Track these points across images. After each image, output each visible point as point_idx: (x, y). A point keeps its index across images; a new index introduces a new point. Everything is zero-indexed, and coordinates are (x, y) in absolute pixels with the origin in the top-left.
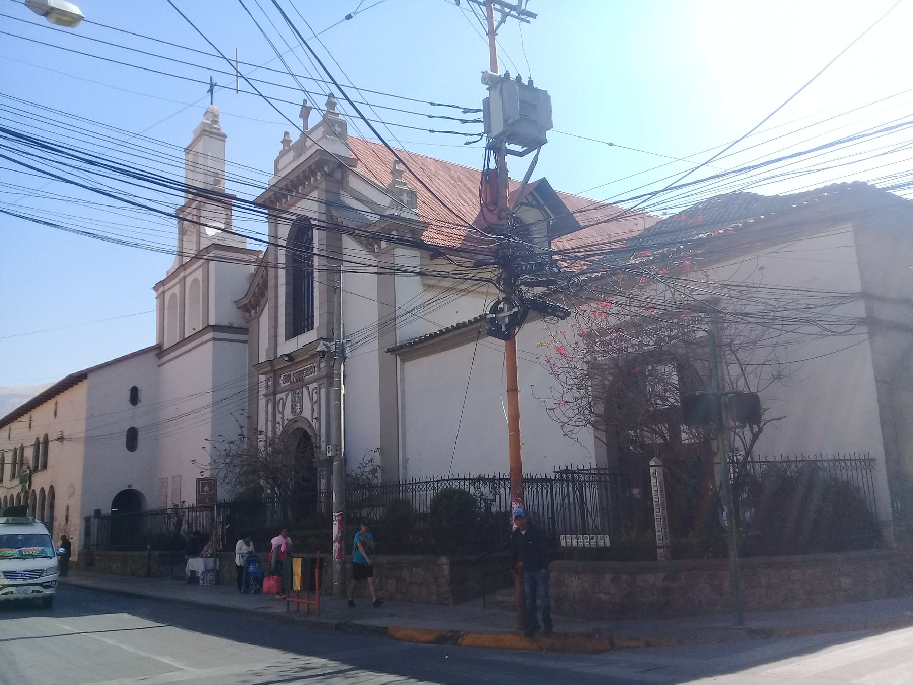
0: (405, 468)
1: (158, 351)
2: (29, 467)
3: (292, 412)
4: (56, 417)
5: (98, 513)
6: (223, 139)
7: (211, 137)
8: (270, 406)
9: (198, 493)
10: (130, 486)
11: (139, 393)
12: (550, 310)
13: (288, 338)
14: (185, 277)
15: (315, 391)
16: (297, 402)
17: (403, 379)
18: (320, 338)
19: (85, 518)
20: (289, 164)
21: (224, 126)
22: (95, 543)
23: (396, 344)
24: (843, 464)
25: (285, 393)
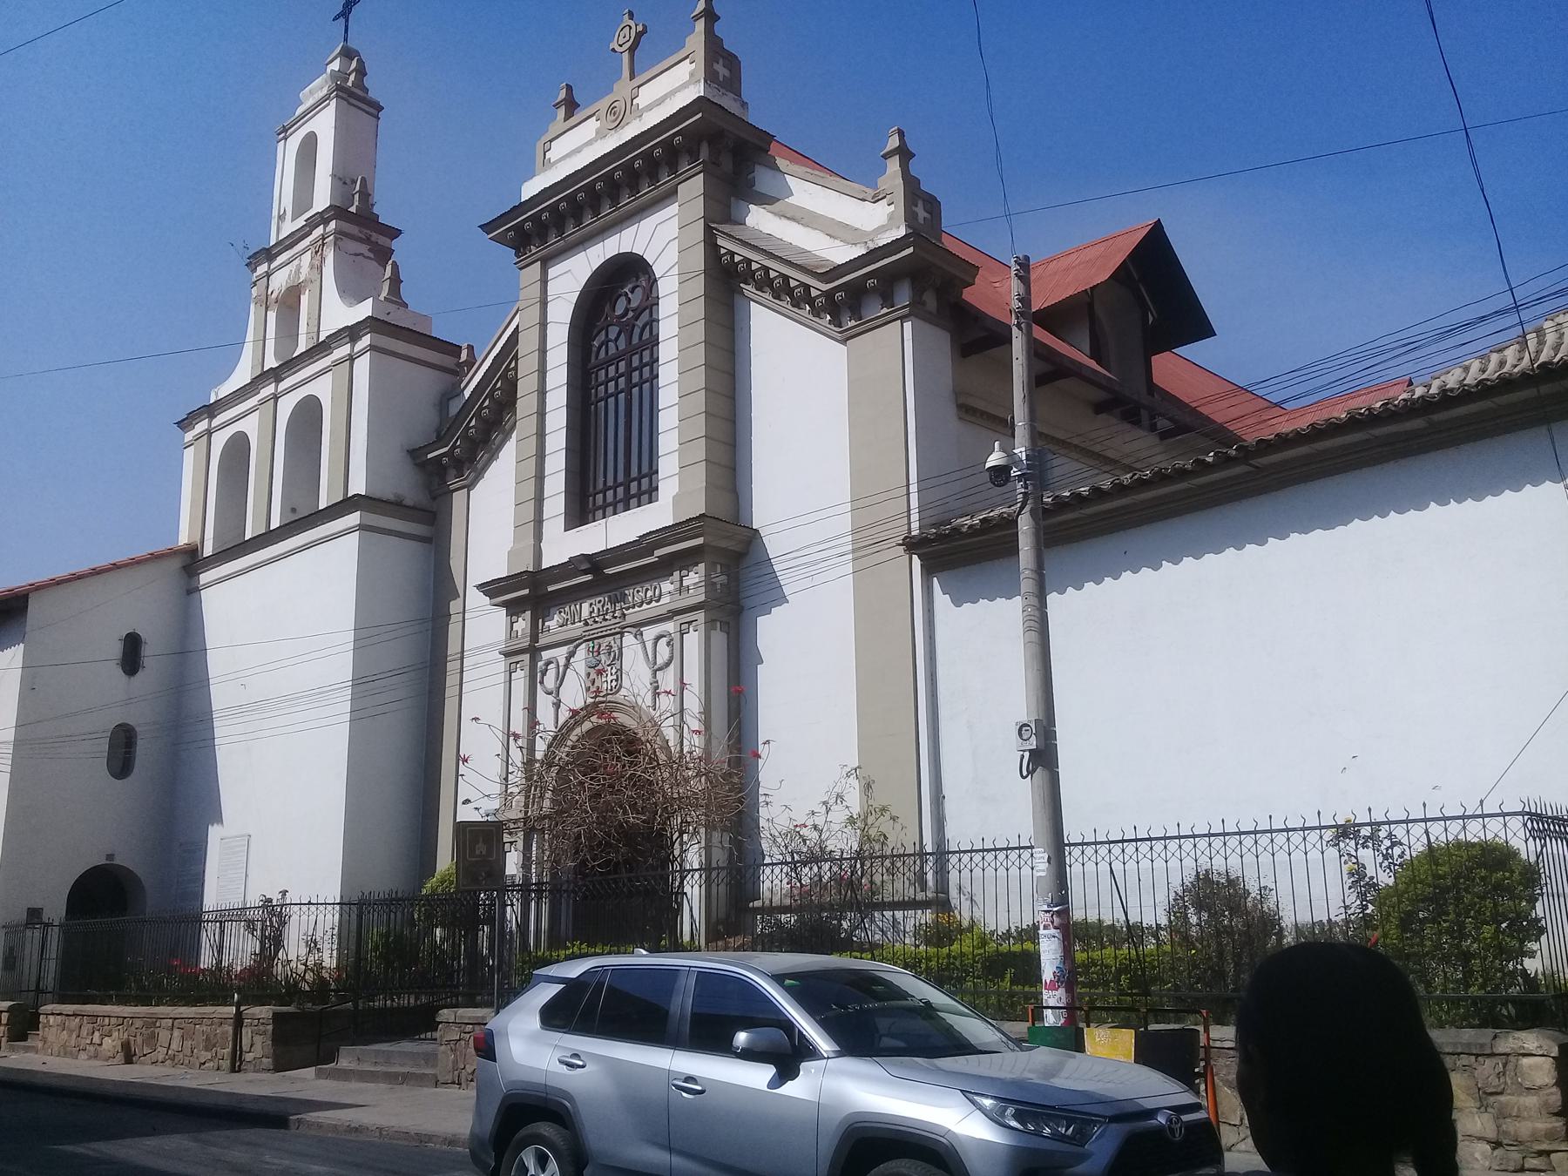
1: (192, 562)
3: (588, 689)
5: (34, 914)
7: (349, 103)
8: (520, 679)
10: (110, 857)
13: (569, 526)
15: (663, 641)
16: (606, 662)
18: (702, 515)
19: (4, 927)
20: (589, 143)
21: (376, 88)
22: (33, 987)
23: (909, 529)
25: (564, 650)
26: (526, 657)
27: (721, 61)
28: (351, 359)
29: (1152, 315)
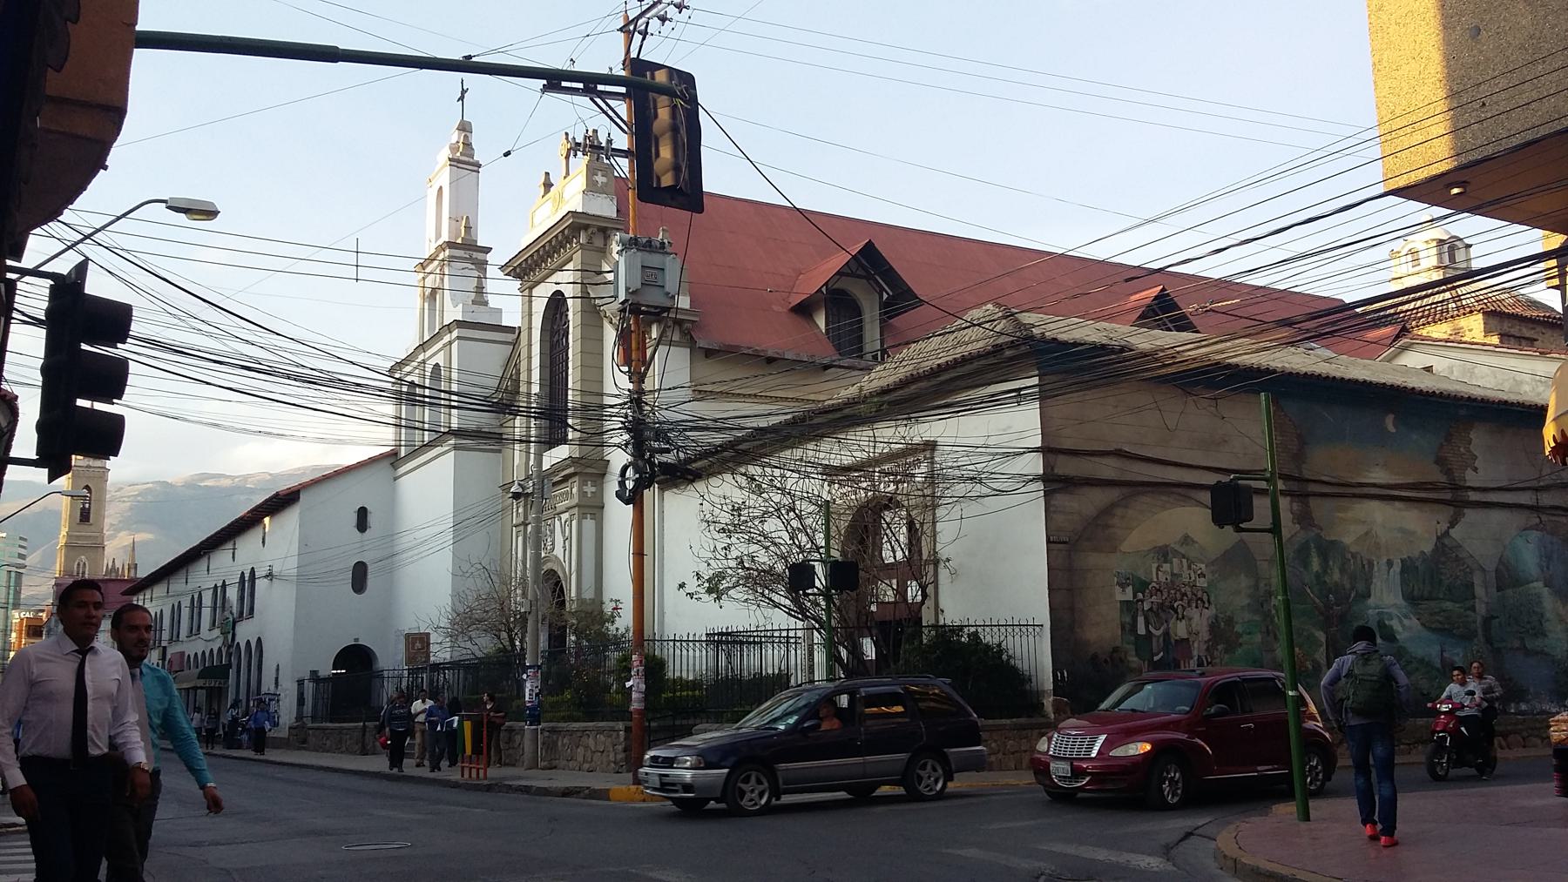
0: (662, 623)
1: (392, 459)
2: (231, 613)
4: (264, 546)
5: (314, 673)
6: (476, 168)
7: (458, 167)
8: (520, 539)
9: (407, 649)
10: (356, 640)
11: (369, 514)
12: (679, 474)
14: (424, 362)
17: (662, 512)
19: (298, 681)
24: (1031, 629)
26: (522, 528)
27: (600, 173)
28: (450, 343)
29: (888, 294)
